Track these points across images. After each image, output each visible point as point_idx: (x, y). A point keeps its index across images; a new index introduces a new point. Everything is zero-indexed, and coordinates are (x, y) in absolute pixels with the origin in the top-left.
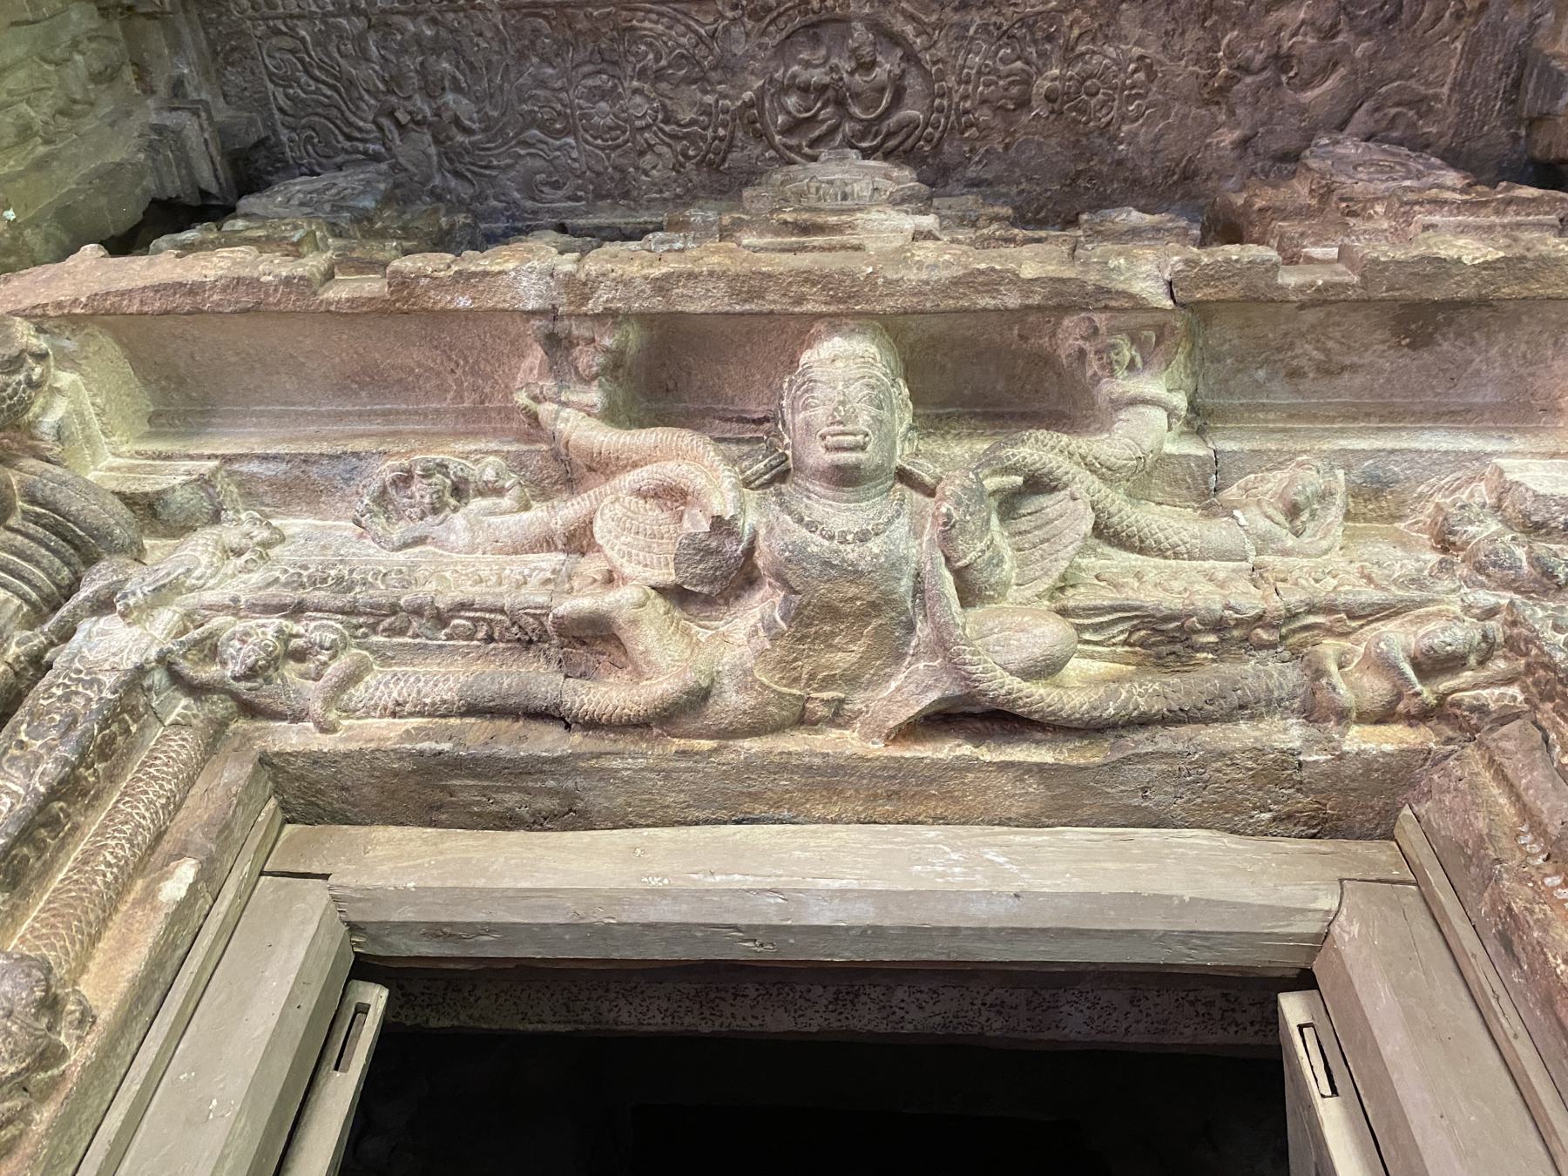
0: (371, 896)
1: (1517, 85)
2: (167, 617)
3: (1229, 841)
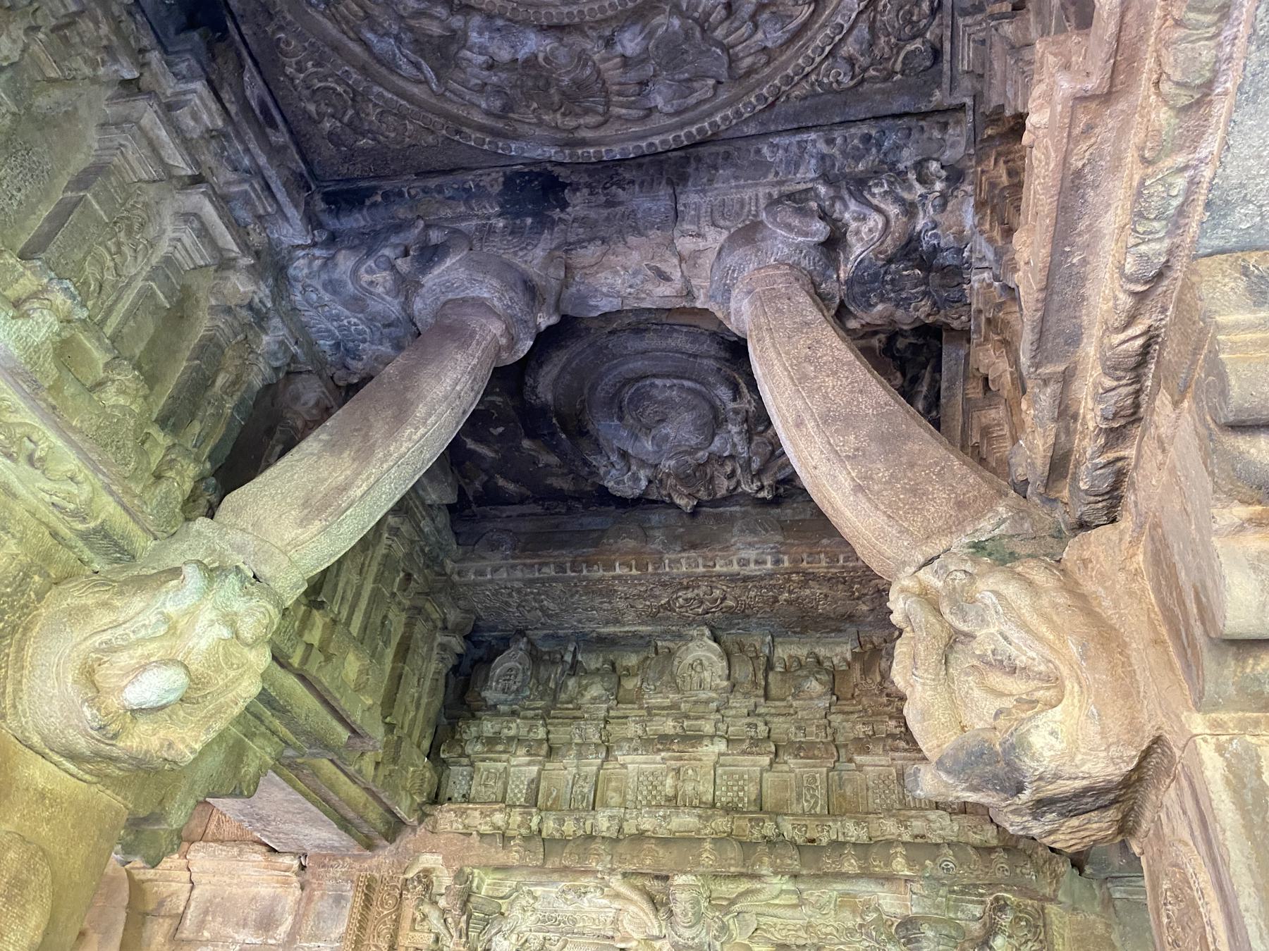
2: (514, 937)
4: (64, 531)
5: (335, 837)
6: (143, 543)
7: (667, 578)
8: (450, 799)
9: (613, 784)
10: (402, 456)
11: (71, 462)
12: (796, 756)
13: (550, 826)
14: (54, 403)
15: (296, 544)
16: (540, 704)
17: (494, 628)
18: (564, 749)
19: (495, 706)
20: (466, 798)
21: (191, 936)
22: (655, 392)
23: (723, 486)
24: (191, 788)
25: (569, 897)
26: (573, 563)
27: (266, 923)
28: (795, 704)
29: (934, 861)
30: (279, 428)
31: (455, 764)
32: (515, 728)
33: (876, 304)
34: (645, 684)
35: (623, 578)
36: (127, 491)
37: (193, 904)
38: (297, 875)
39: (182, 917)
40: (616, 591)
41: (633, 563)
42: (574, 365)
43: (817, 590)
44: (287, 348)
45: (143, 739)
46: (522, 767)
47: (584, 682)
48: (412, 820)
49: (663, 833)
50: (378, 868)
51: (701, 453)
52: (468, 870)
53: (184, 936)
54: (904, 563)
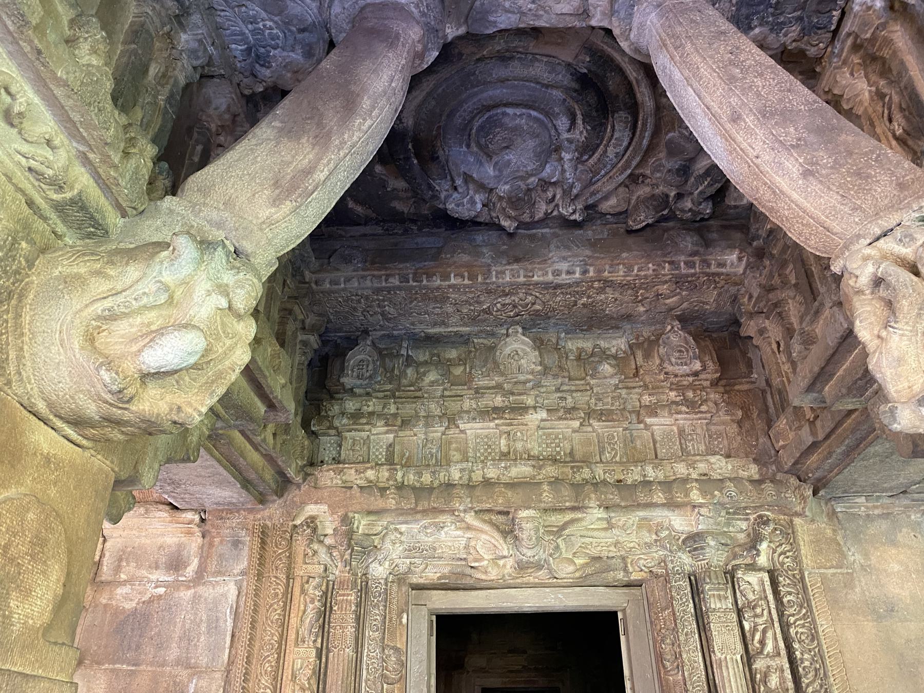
0: (437, 609)
1: (734, 301)
2: (387, 563)
3: (608, 590)
4: (39, 200)
5: (235, 495)
6: (113, 220)
7: (493, 287)
8: (322, 462)
9: (454, 445)
10: (353, 146)
11: (45, 123)
12: (599, 420)
13: (411, 478)
14: (40, 46)
15: (270, 223)
16: (389, 387)
17: (340, 330)
18: (414, 421)
19: (352, 389)
20: (337, 460)
21: (110, 579)
22: (506, 120)
23: (542, 208)
24: (155, 454)
25: (428, 531)
26: (415, 274)
27: (176, 563)
28: (592, 382)
29: (721, 491)
30: (196, 129)
31: (324, 434)
32: (372, 405)
33: (756, 26)
34: (473, 371)
35: (460, 283)
36: (106, 159)
37: (107, 554)
38: (199, 526)
39: (99, 564)
40: (449, 298)
41: (466, 274)
42: (440, 90)
43: (610, 294)
44: (205, 49)
45: (153, 403)
46: (380, 435)
47: (422, 370)
48: (299, 479)
49: (505, 479)
50: (270, 518)
51: (532, 179)
52: (351, 515)
53: (103, 579)
54: (858, 236)
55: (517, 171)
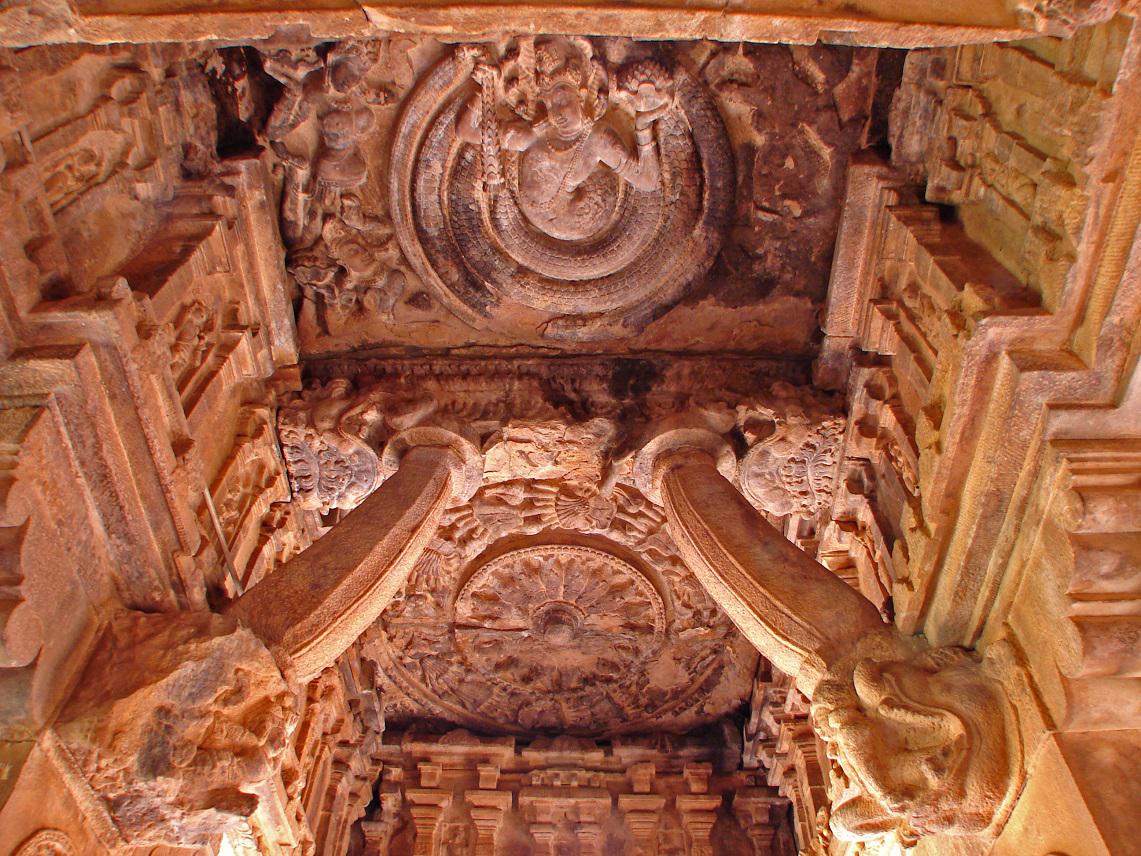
55: (563, 162)
